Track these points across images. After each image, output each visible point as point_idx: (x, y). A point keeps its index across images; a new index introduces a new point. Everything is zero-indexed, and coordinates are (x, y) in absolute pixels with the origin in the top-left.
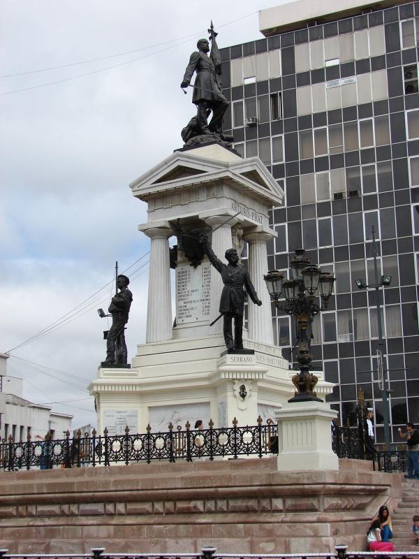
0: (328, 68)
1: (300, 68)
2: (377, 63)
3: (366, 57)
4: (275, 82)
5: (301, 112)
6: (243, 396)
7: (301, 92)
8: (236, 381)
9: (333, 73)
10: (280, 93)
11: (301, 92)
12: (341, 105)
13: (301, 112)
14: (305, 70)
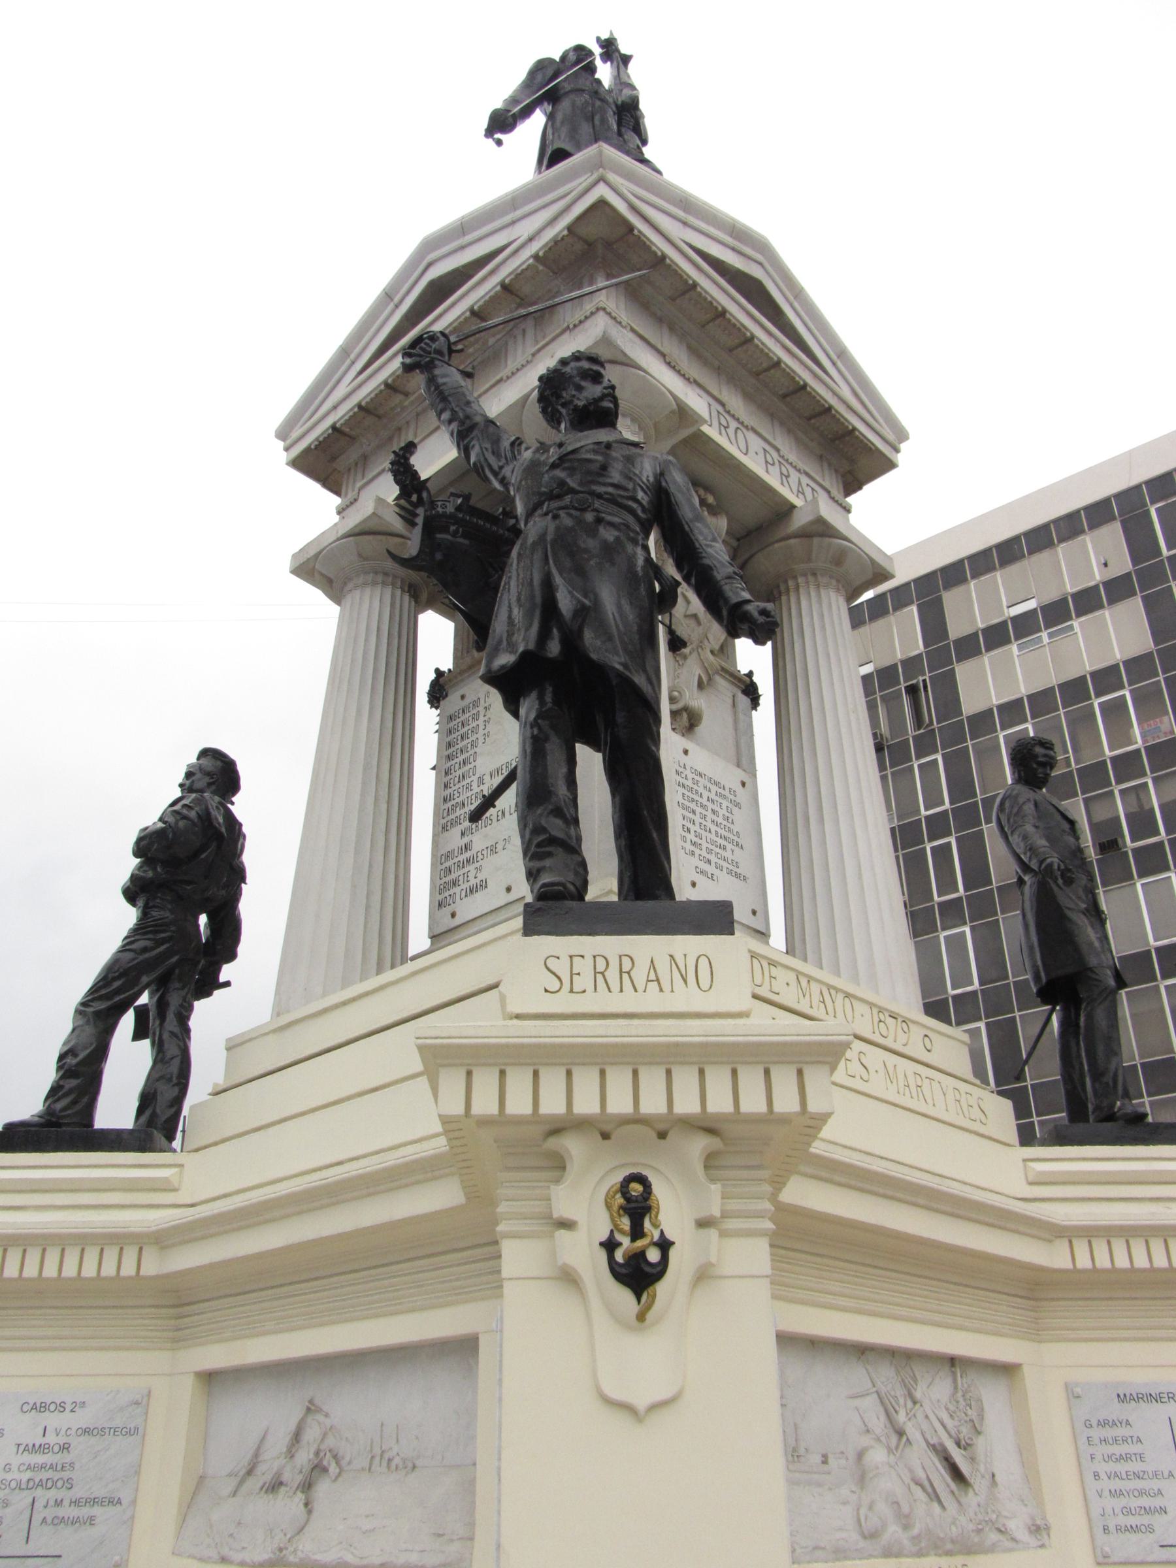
0: (1012, 619)
1: (956, 629)
2: (1117, 589)
3: (1092, 584)
4: (912, 664)
5: (970, 705)
6: (639, 1275)
7: (963, 672)
8: (574, 1146)
9: (1025, 626)
10: (924, 681)
11: (963, 672)
12: (1053, 679)
13: (970, 705)
14: (969, 630)
